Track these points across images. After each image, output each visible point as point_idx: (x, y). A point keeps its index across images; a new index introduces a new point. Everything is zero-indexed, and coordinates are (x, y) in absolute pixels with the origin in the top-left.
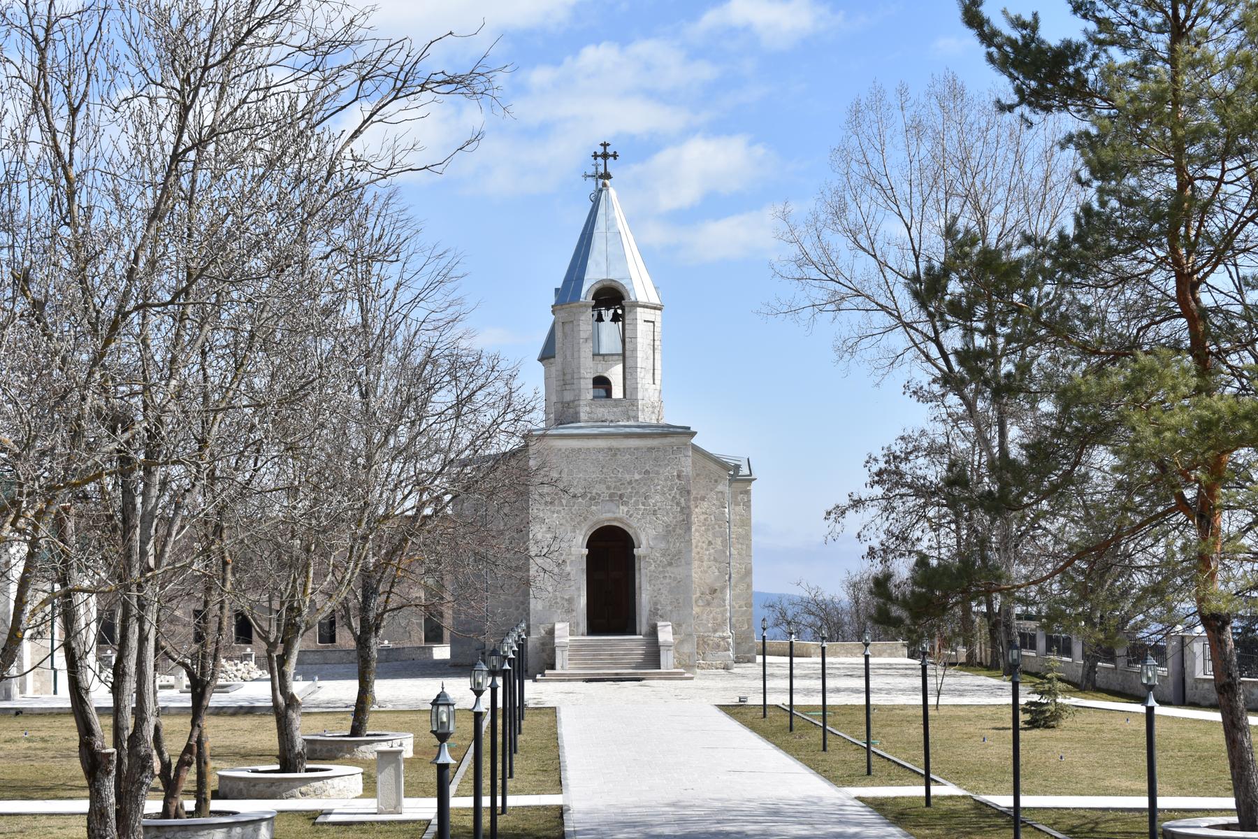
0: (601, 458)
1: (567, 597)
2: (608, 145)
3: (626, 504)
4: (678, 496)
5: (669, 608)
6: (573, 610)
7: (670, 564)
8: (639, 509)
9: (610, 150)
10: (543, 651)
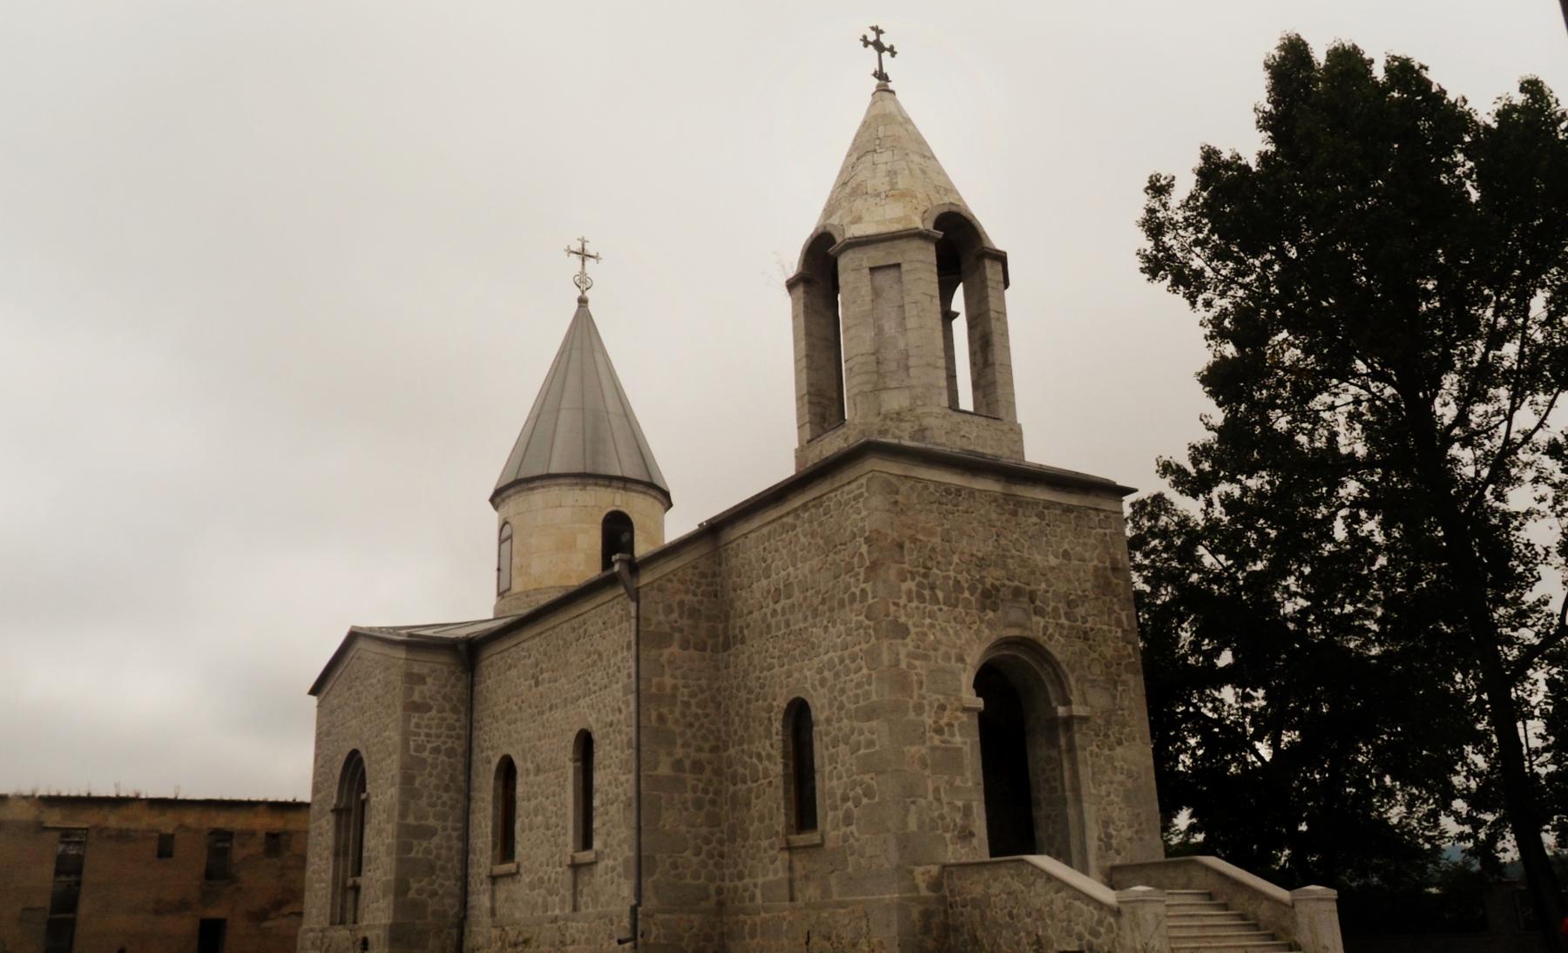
1: (960, 804)
2: (882, 32)
3: (1039, 612)
4: (1116, 608)
5: (1126, 833)
6: (972, 834)
7: (1120, 743)
8: (1062, 626)
9: (886, 40)
10: (926, 930)
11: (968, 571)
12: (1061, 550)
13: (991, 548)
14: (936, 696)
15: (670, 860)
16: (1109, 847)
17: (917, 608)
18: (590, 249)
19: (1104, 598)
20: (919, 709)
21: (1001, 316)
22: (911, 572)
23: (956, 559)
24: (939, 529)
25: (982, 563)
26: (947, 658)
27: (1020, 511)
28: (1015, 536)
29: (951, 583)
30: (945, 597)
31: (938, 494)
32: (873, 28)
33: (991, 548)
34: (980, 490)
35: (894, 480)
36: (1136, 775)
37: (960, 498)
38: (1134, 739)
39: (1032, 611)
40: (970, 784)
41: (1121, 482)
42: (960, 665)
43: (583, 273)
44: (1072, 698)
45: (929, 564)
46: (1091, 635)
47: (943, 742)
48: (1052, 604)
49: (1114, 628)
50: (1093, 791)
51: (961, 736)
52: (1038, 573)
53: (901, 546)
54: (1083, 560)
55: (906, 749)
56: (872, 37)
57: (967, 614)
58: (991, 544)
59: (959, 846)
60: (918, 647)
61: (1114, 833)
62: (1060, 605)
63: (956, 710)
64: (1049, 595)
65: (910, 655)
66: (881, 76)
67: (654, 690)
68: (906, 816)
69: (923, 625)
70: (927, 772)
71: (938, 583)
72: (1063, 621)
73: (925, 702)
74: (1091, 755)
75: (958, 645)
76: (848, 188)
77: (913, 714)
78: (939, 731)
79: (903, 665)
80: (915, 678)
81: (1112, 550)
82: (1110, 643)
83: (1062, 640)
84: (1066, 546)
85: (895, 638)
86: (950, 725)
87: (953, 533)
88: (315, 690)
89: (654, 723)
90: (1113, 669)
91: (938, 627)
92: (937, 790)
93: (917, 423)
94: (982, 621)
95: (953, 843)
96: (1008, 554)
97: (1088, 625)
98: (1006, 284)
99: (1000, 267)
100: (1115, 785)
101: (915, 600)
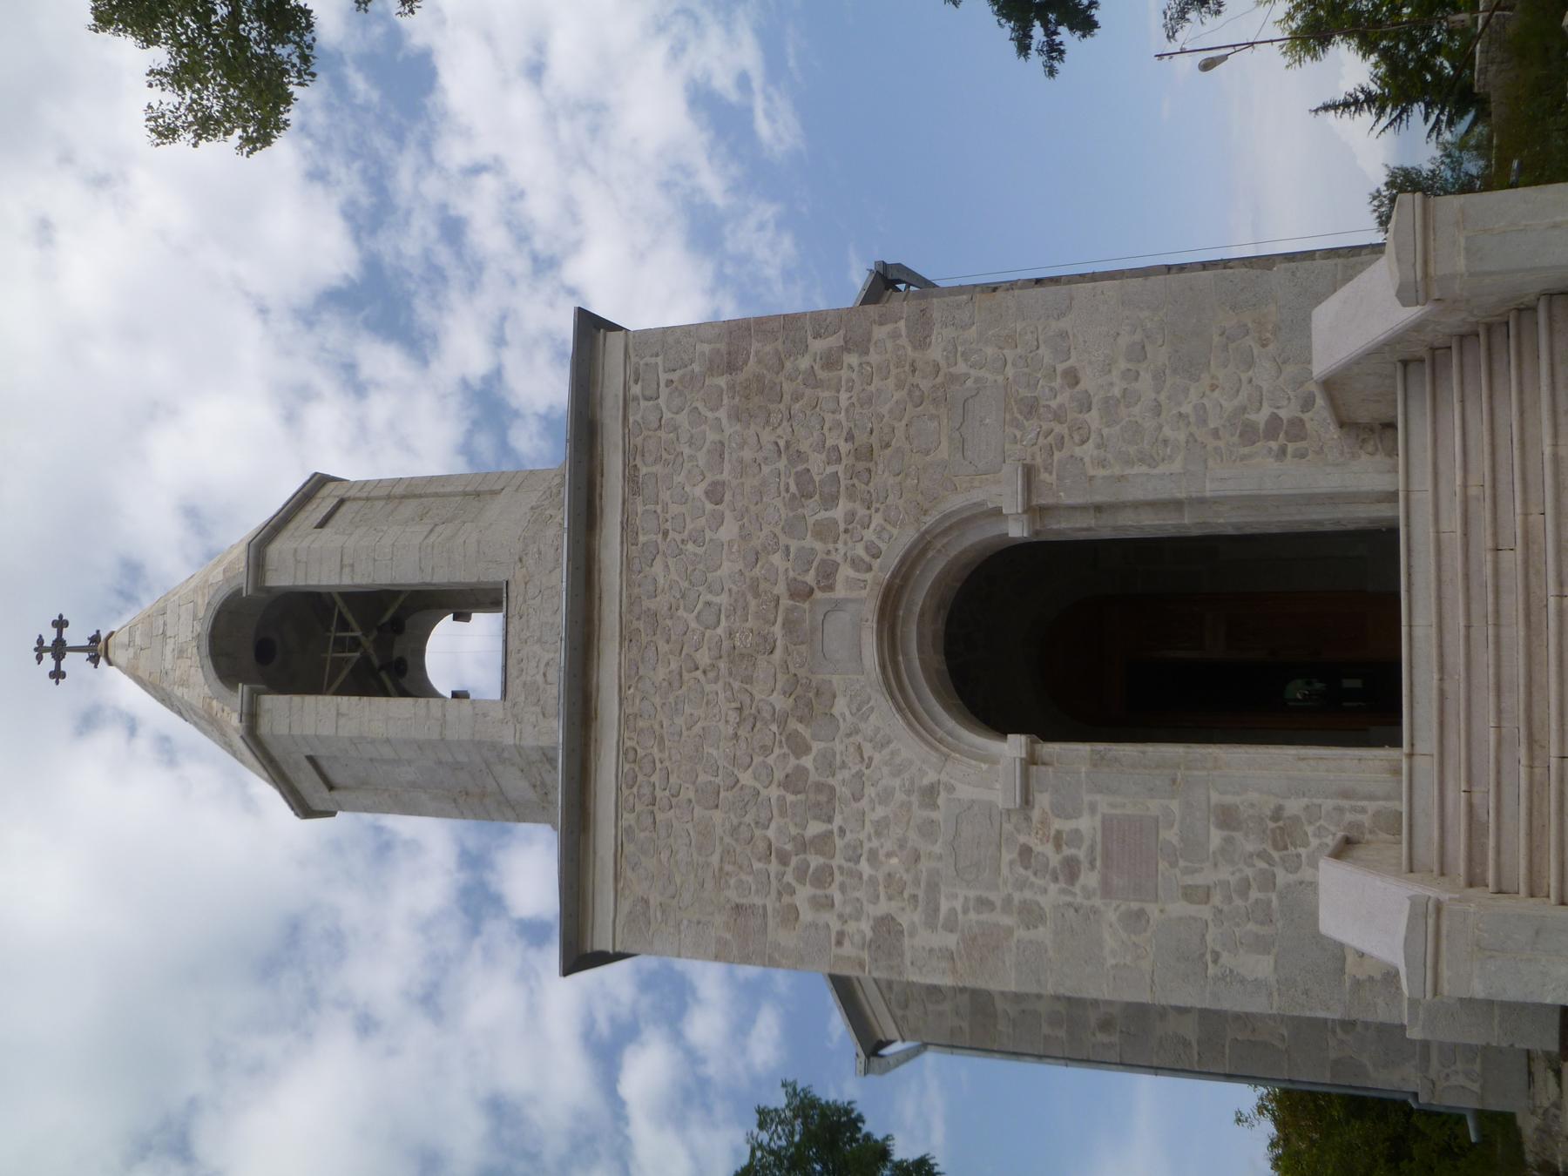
0: (662, 672)
2: (40, 641)
3: (828, 574)
4: (804, 363)
6: (1277, 814)
7: (1072, 378)
8: (851, 516)
11: (766, 750)
12: (709, 506)
13: (719, 687)
14: (1005, 870)
15: (1338, 1030)
16: (1297, 430)
17: (843, 888)
19: (787, 397)
20: (1031, 915)
21: (346, 561)
22: (780, 894)
23: (746, 778)
24: (698, 811)
25: (748, 716)
26: (928, 830)
27: (646, 604)
28: (693, 625)
29: (790, 798)
30: (816, 818)
31: (637, 809)
32: (39, 659)
33: (719, 687)
34: (621, 704)
35: (625, 906)
36: (1138, 337)
37: (641, 752)
38: (1064, 335)
39: (827, 595)
40: (1175, 805)
42: (941, 801)
44: (990, 505)
45: (762, 846)
46: (861, 438)
47: (1093, 867)
48: (809, 542)
49: (844, 373)
50: (1176, 467)
51: (1076, 814)
52: (757, 572)
53: (738, 908)
54: (719, 451)
55: (1111, 961)
57: (844, 765)
58: (714, 687)
59: (1302, 851)
60: (914, 897)
61: (1266, 412)
62: (811, 521)
63: (1028, 819)
64: (794, 545)
65: (931, 925)
67: (1062, 1033)
68: (1242, 981)
69: (873, 881)
70: (1153, 910)
71: (793, 831)
72: (838, 513)
73: (1017, 896)
74: (1102, 463)
75: (904, 797)
77: (1041, 929)
78: (1071, 870)
79: (951, 940)
80: (973, 916)
81: (696, 367)
82: (872, 388)
83: (877, 520)
84: (699, 491)
85: (902, 955)
86: (1058, 840)
87: (703, 778)
89: (1115, 1038)
90: (925, 385)
91: (875, 843)
92: (1189, 894)
93: (540, 765)
94: (856, 731)
95: (1298, 868)
96: (726, 644)
97: (844, 447)
99: (274, 549)
100: (1162, 397)
101: (828, 892)
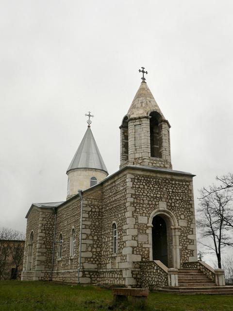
9: (145, 70)
18: (91, 114)
41: (192, 174)
43: (89, 120)
56: (142, 70)
66: (143, 79)
76: (133, 106)
88: (26, 217)
98: (169, 127)
